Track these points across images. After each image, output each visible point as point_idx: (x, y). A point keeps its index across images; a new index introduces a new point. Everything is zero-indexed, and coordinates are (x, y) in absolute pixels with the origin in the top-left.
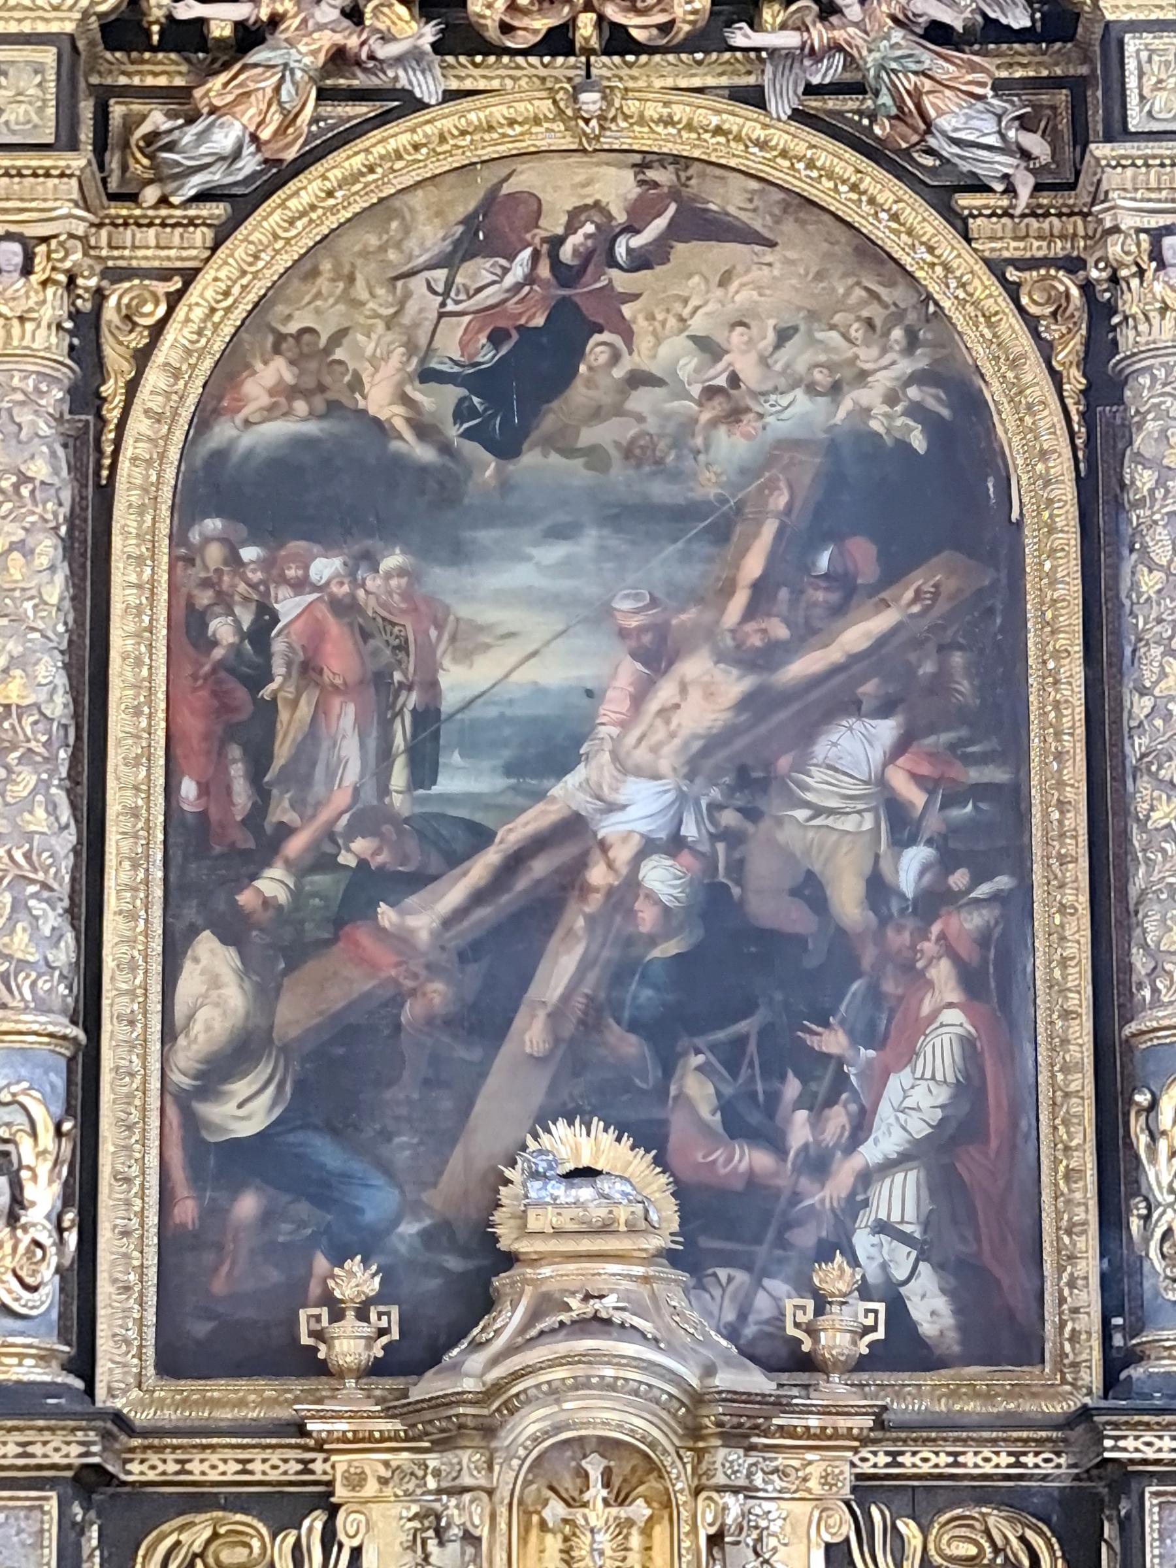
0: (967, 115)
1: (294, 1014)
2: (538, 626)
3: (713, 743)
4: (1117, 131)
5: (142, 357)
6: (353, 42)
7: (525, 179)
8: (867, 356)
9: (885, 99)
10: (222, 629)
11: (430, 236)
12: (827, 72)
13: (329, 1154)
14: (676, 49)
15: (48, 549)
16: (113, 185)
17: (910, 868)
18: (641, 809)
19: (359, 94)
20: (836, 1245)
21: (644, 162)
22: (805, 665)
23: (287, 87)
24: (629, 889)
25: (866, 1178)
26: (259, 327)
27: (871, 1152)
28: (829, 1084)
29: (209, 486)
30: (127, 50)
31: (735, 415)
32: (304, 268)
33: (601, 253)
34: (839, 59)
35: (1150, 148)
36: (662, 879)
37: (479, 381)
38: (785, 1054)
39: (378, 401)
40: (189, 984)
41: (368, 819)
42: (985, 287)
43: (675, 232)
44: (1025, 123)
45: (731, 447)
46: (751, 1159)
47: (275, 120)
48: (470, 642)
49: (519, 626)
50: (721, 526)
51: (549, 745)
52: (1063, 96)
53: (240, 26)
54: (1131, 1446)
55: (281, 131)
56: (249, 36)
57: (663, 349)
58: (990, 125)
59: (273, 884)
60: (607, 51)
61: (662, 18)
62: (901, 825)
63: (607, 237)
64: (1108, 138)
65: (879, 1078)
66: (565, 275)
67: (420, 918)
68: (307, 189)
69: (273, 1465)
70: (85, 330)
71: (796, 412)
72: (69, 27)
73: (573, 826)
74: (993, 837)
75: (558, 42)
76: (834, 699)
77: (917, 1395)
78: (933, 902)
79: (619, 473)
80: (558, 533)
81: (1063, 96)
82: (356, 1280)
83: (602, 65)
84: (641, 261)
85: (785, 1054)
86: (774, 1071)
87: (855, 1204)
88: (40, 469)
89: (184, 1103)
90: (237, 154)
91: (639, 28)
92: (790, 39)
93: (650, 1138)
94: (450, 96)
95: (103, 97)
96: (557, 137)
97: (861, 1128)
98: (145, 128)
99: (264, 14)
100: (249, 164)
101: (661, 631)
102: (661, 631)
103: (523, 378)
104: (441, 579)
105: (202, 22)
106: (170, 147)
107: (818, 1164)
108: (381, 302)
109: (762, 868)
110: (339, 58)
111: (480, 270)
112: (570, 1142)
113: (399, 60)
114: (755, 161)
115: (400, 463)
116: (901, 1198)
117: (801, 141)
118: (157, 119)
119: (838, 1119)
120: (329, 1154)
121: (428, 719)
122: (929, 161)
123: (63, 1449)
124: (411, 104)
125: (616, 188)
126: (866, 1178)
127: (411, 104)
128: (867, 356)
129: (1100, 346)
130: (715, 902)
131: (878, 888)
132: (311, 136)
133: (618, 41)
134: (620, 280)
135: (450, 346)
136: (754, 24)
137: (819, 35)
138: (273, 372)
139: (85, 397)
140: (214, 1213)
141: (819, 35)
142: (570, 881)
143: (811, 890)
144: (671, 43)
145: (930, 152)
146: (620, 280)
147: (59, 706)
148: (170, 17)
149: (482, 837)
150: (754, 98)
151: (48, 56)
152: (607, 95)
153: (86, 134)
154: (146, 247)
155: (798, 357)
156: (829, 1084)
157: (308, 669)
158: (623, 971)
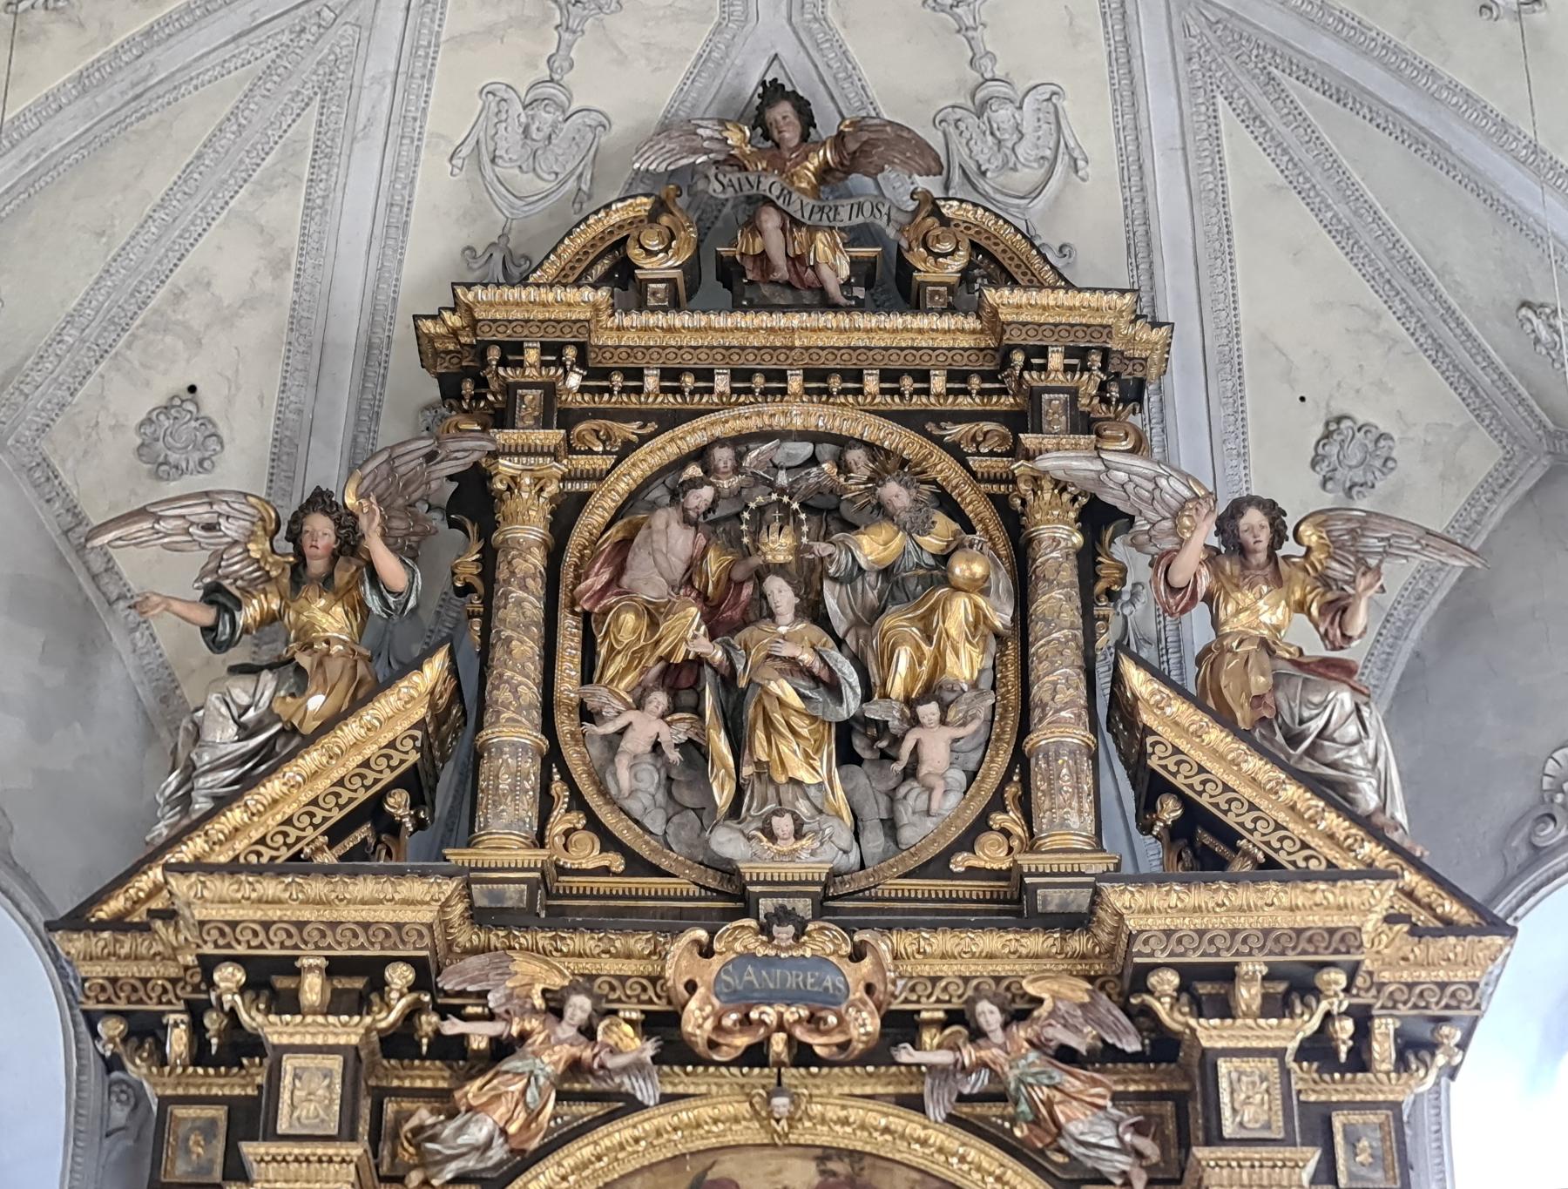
4: (1214, 1137)
6: (587, 1054)
9: (1024, 1107)
12: (976, 1083)
14: (851, 1064)
16: (384, 1170)
21: (825, 1155)
23: (532, 1093)
30: (400, 1058)
34: (985, 1074)
35: (1241, 1153)
44: (1138, 1129)
47: (521, 1116)
52: (1169, 1107)
53: (494, 1041)
55: (526, 1126)
56: (502, 1049)
58: (1109, 1130)
60: (796, 1064)
61: (839, 1038)
64: (1208, 1143)
72: (354, 1040)
75: (755, 1056)
81: (1169, 1107)
83: (791, 1075)
90: (488, 1145)
91: (820, 1044)
92: (945, 1057)
94: (666, 1099)
95: (379, 1096)
96: (750, 1132)
98: (414, 1122)
99: (515, 1031)
100: (498, 1153)
105: (462, 1038)
106: (433, 1139)
110: (576, 1067)
113: (625, 1070)
114: (916, 1155)
117: (955, 1140)
118: (424, 1115)
122: (1059, 1158)
124: (633, 1105)
127: (633, 1105)
132: (550, 1131)
133: (803, 1056)
136: (917, 1044)
137: (969, 1055)
141: (969, 1055)
144: (847, 1058)
145: (1061, 1150)
148: (437, 1032)
150: (915, 1104)
151: (335, 1063)
152: (795, 1100)
153: (363, 1128)
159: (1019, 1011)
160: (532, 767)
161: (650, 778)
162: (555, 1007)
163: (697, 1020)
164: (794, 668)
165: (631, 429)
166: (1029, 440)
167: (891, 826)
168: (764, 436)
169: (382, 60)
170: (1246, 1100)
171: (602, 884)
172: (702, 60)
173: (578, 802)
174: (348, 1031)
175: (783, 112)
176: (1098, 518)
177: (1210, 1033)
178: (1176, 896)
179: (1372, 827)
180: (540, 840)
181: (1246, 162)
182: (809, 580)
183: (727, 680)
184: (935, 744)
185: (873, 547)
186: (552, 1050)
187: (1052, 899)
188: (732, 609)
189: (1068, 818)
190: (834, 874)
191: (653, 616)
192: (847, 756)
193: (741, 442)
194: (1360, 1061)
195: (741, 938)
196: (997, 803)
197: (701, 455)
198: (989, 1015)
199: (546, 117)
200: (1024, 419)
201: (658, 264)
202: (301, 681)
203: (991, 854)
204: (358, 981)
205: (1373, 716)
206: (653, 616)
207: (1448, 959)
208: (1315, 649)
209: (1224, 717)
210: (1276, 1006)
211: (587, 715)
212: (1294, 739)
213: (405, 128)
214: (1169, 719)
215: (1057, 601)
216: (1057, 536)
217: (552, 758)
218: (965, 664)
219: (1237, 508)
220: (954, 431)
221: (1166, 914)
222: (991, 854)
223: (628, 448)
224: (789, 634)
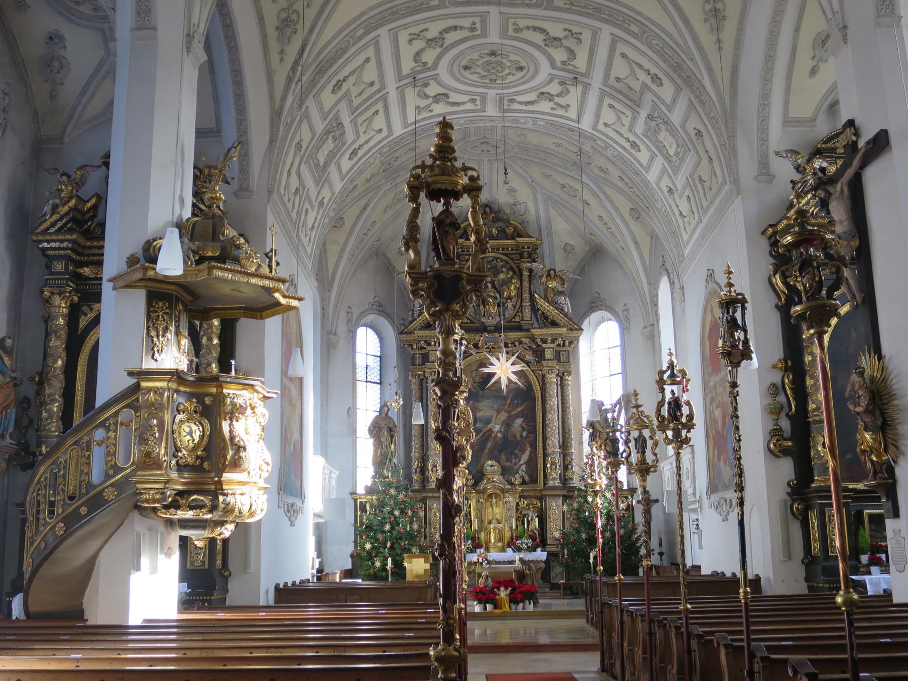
3: (504, 421)
11: (474, 367)
17: (524, 434)
18: (497, 428)
22: (513, 413)
24: (496, 436)
28: (516, 456)
36: (499, 435)
37: (480, 383)
38: (512, 453)
46: (508, 464)
51: (488, 421)
54: (545, 493)
62: (523, 428)
73: (490, 430)
74: (533, 430)
76: (517, 416)
77: (526, 487)
78: (527, 437)
85: (512, 453)
93: (498, 462)
104: (476, 404)
107: (515, 464)
112: (490, 462)
116: (523, 468)
129: (543, 380)
130: (505, 437)
131: (521, 436)
135: (477, 379)
143: (514, 436)
156: (516, 456)
159: (521, 343)
163: (480, 344)
164: (490, 296)
167: (504, 315)
170: (549, 354)
175: (487, 209)
176: (531, 271)
177: (544, 346)
178: (540, 330)
179: (566, 315)
181: (553, 213)
182: (493, 283)
185: (501, 276)
187: (525, 327)
192: (499, 305)
194: (564, 345)
198: (517, 343)
200: (521, 255)
203: (517, 319)
207: (574, 334)
208: (560, 289)
209: (548, 302)
210: (553, 341)
214: (541, 302)
215: (526, 284)
216: (526, 274)
218: (513, 294)
219: (550, 270)
220: (512, 256)
221: (537, 332)
222: (517, 319)
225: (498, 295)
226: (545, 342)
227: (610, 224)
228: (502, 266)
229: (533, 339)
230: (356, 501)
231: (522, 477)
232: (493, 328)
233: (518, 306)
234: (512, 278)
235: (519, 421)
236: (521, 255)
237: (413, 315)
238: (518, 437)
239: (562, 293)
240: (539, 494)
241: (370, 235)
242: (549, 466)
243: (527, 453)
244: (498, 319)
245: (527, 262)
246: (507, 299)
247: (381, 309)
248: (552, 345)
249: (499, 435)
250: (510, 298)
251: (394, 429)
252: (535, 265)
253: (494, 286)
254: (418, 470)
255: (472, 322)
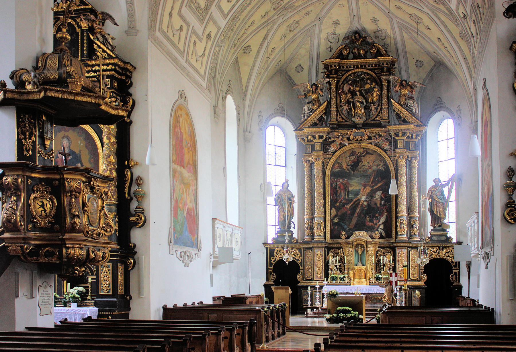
0: (387, 147)
1: (339, 214)
2: (356, 184)
3: (369, 193)
5: (327, 165)
7: (355, 150)
8: (380, 163)
10: (333, 185)
11: (348, 155)
13: (342, 224)
15: (321, 181)
17: (383, 202)
18: (364, 198)
19: (342, 145)
20: (378, 230)
21: (364, 148)
25: (380, 225)
26: (336, 162)
27: (380, 223)
28: (377, 218)
29: (332, 174)
31: (370, 168)
32: (339, 157)
33: (360, 156)
36: (365, 203)
37: (352, 166)
38: (374, 216)
39: (344, 167)
40: (332, 211)
41: (344, 199)
42: (389, 158)
43: (366, 154)
45: (370, 171)
46: (371, 224)
48: (351, 186)
49: (355, 185)
50: (369, 177)
51: (357, 193)
54: (396, 245)
57: (366, 163)
59: (338, 204)
62: (382, 199)
63: (361, 154)
65: (380, 218)
66: (358, 157)
67: (348, 206)
68: (339, 152)
69: (338, 246)
70: (323, 165)
71: (375, 168)
73: (359, 199)
75: (357, 140)
76: (378, 190)
78: (385, 205)
79: (362, 172)
80: (358, 177)
82: (344, 233)
84: (363, 156)
85: (374, 216)
86: (373, 218)
87: (379, 227)
88: (320, 175)
89: (332, 220)
97: (379, 221)
101: (365, 185)
102: (365, 185)
103: (355, 165)
104: (349, 181)
107: (376, 224)
108: (344, 160)
109: (372, 202)
111: (352, 157)
115: (346, 172)
116: (382, 226)
119: (377, 221)
120: (342, 224)
121: (348, 192)
123: (324, 245)
125: (362, 150)
126: (380, 225)
128: (380, 163)
129: (396, 164)
130: (369, 205)
131: (381, 204)
134: (362, 158)
138: (337, 165)
139: (323, 168)
140: (334, 228)
142: (359, 204)
143: (376, 204)
146: (362, 158)
147: (322, 192)
149: (352, 200)
150: (371, 143)
154: (328, 156)
155: (375, 163)
157: (340, 188)
158: (363, 210)
159: (380, 136)
160: (336, 112)
161: (346, 112)
162: (338, 137)
163: (351, 138)
165: (343, 72)
166: (382, 73)
167: (369, 115)
168: (357, 72)
169: (317, 32)
171: (343, 123)
172: (349, 28)
173: (340, 115)
174: (321, 141)
175: (357, 35)
180: (337, 120)
182: (360, 91)
183: (353, 102)
184: (373, 108)
186: (338, 141)
187: (384, 124)
188: (353, 94)
189: (385, 114)
190: (364, 122)
191: (346, 95)
193: (354, 73)
194: (412, 137)
195: (355, 130)
196: (379, 113)
197: (350, 75)
199: (333, 36)
201: (345, 52)
202: (314, 105)
203: (378, 118)
204: (321, 137)
205: (415, 103)
206: (346, 95)
208: (410, 96)
211: (341, 106)
212: (407, 106)
213: (319, 38)
215: (385, 92)
217: (337, 111)
218: (375, 99)
220: (376, 71)
222: (378, 118)
223: (343, 75)
224: (359, 98)
225: (364, 101)
226: (397, 135)
227: (446, 45)
228: (368, 79)
229: (388, 132)
230: (267, 249)
231: (381, 234)
232: (361, 125)
233: (379, 109)
234: (374, 87)
235: (379, 193)
236: (382, 70)
237: (304, 117)
238: (378, 205)
239: (412, 98)
240: (391, 245)
241: (271, 58)
242: (399, 226)
243: (385, 216)
244: (364, 118)
245: (386, 75)
246: (371, 103)
247: (282, 112)
248: (403, 138)
249: (365, 203)
250: (373, 103)
251: (292, 199)
252: (391, 78)
253: (361, 94)
254: (309, 228)
255: (346, 121)
